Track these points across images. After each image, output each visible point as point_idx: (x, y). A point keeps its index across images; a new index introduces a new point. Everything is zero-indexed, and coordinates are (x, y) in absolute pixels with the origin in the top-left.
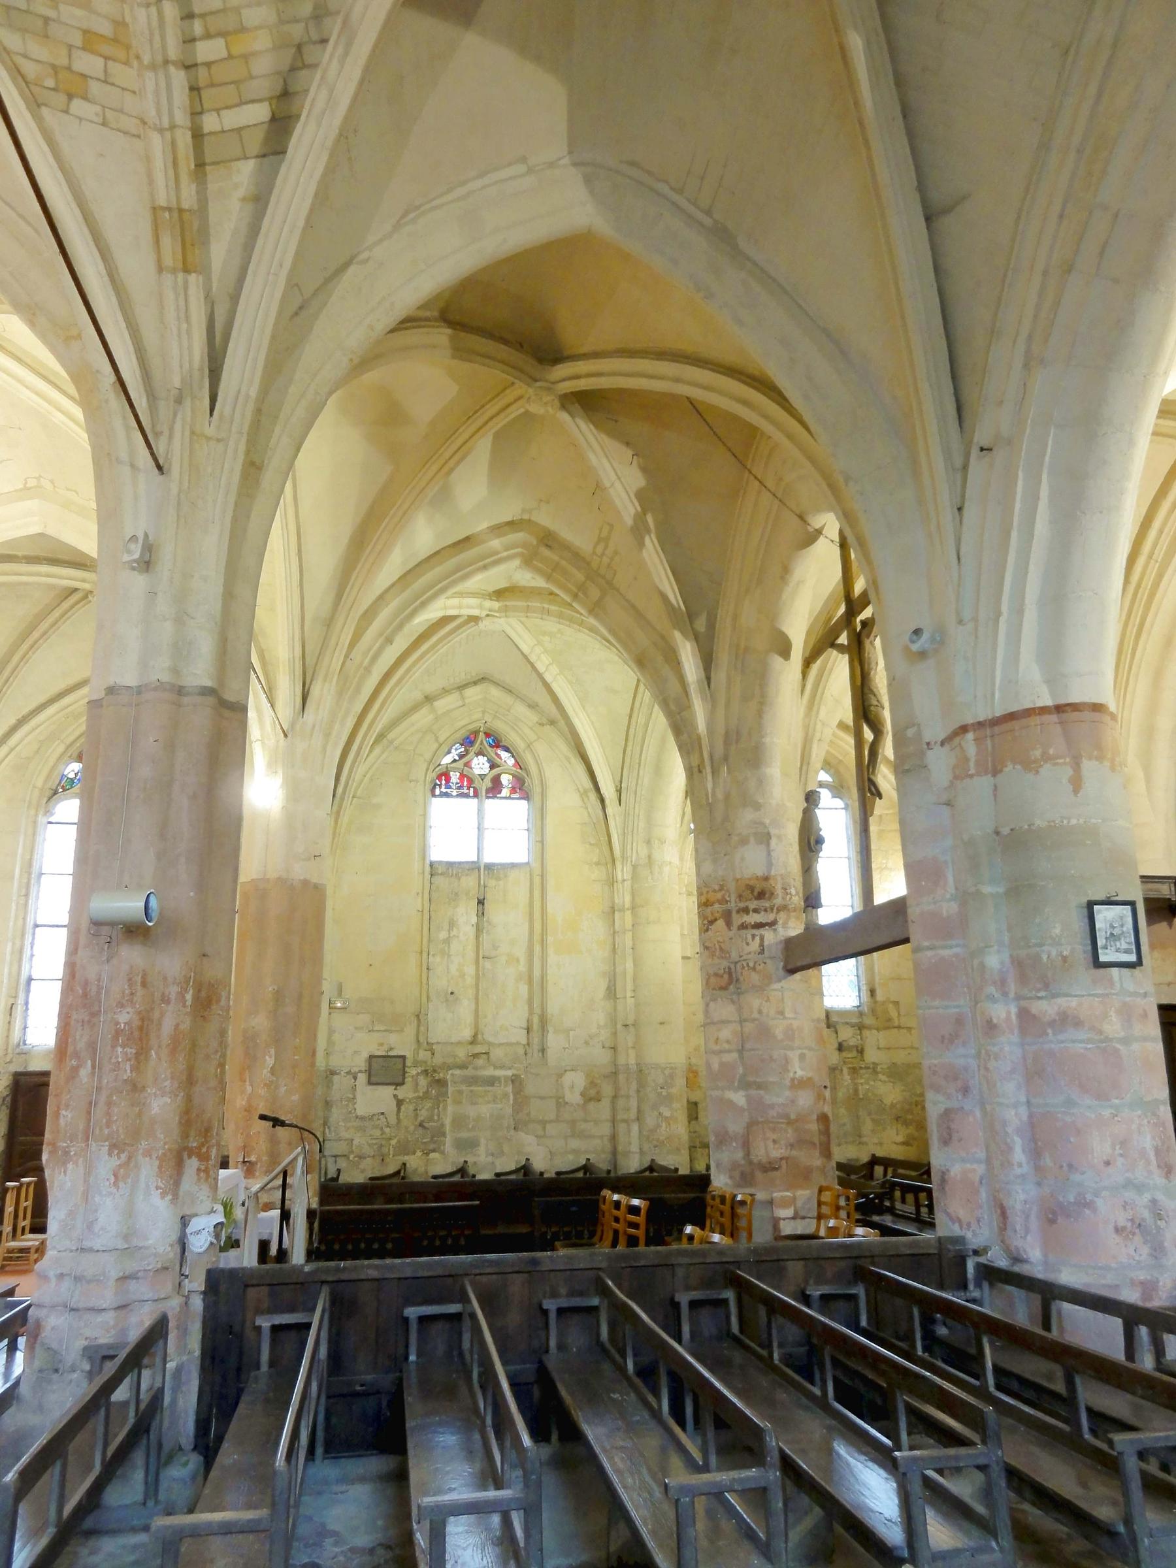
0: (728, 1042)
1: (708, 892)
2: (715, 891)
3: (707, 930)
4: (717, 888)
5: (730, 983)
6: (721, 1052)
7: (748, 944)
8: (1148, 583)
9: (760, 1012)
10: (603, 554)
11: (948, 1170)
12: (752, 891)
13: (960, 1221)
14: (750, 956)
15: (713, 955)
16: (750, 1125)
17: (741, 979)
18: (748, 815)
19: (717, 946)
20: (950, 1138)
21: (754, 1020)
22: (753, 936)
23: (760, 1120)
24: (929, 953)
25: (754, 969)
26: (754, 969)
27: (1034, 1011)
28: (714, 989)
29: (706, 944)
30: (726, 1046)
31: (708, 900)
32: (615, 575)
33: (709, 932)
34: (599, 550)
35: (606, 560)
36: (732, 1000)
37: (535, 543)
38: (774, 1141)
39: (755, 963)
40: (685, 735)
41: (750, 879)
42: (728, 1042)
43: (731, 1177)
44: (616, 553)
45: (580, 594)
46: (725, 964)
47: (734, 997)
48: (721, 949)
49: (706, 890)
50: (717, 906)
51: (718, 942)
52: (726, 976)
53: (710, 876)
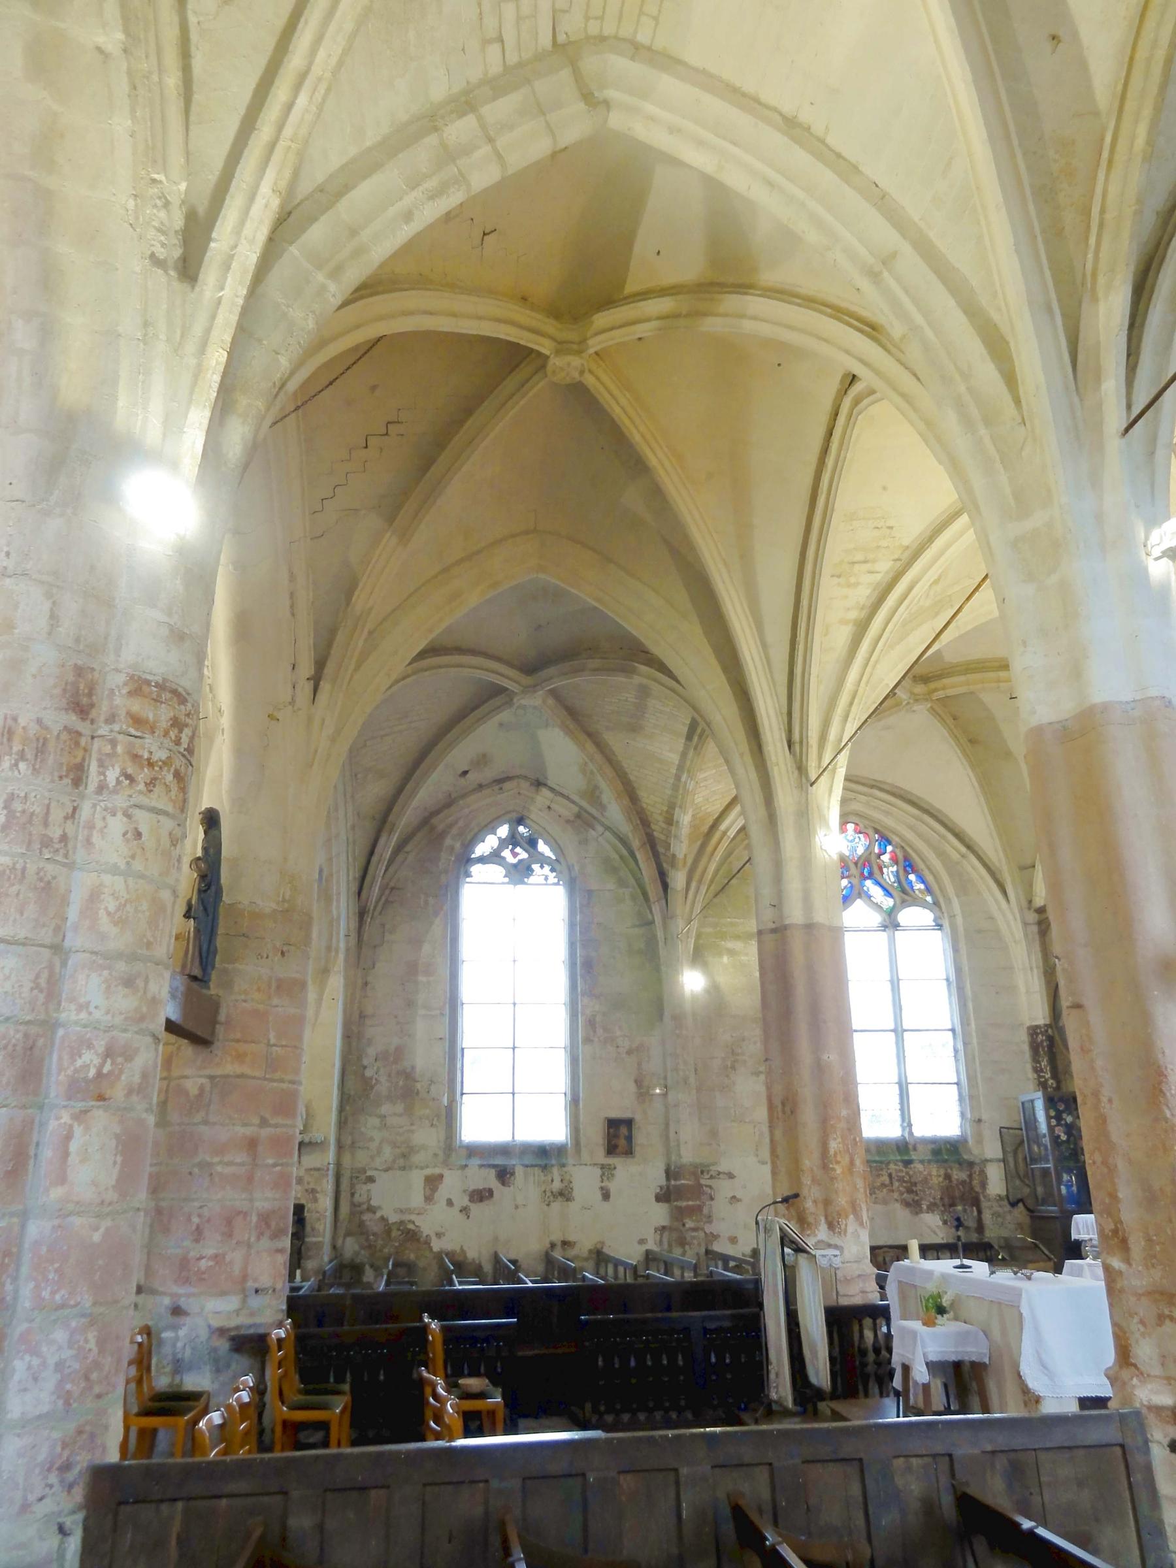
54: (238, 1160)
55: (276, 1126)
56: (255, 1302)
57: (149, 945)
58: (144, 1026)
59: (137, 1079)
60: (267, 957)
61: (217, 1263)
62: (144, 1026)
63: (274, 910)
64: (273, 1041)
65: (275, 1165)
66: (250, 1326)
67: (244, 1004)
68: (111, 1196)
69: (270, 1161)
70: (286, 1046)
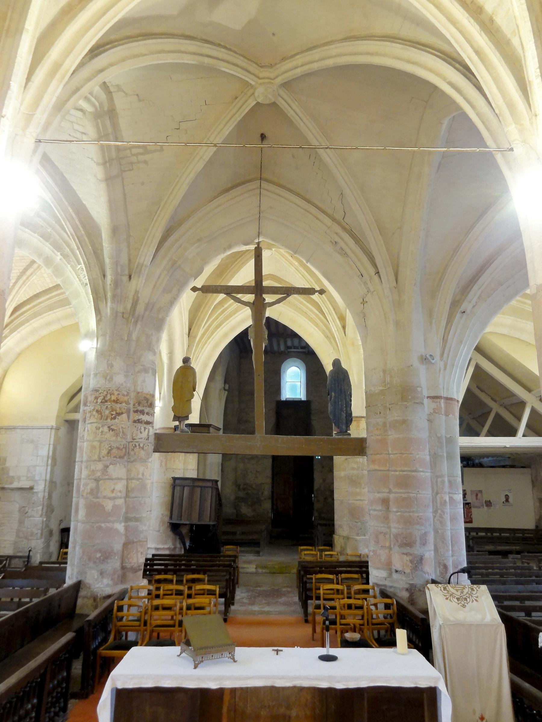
0: (120, 491)
1: (118, 394)
2: (124, 395)
3: (115, 418)
4: (126, 393)
5: (125, 455)
6: (115, 498)
7: (141, 433)
8: (229, 310)
9: (143, 474)
10: (136, 155)
11: (424, 555)
12: (147, 402)
13: (428, 573)
14: (140, 440)
15: (117, 435)
16: (125, 545)
17: (132, 453)
18: (150, 356)
19: (121, 430)
20: (426, 543)
21: (138, 479)
22: (145, 429)
23: (135, 540)
24: (422, 474)
25: (143, 448)
26: (143, 448)
27: (454, 498)
28: (115, 457)
29: (111, 427)
30: (119, 494)
31: (118, 400)
32: (130, 170)
33: (116, 420)
34: (134, 151)
35: (134, 159)
36: (125, 465)
37: (106, 109)
38: (142, 553)
39: (144, 445)
40: (119, 290)
41: (147, 394)
42: (120, 491)
43: (112, 579)
44: (145, 162)
45: (108, 164)
46: (124, 442)
47: (126, 463)
48: (123, 432)
49: (118, 392)
50: (124, 404)
51: (122, 428)
52: (124, 450)
53: (122, 385)
54: (378, 508)
55: (395, 493)
56: (395, 576)
57: (90, 457)
58: (90, 477)
59: (89, 491)
60: (380, 413)
61: (374, 554)
62: (90, 477)
63: (382, 390)
64: (390, 452)
65: (397, 512)
66: (391, 587)
67: (372, 437)
68: (84, 519)
69: (395, 510)
70: (396, 454)
